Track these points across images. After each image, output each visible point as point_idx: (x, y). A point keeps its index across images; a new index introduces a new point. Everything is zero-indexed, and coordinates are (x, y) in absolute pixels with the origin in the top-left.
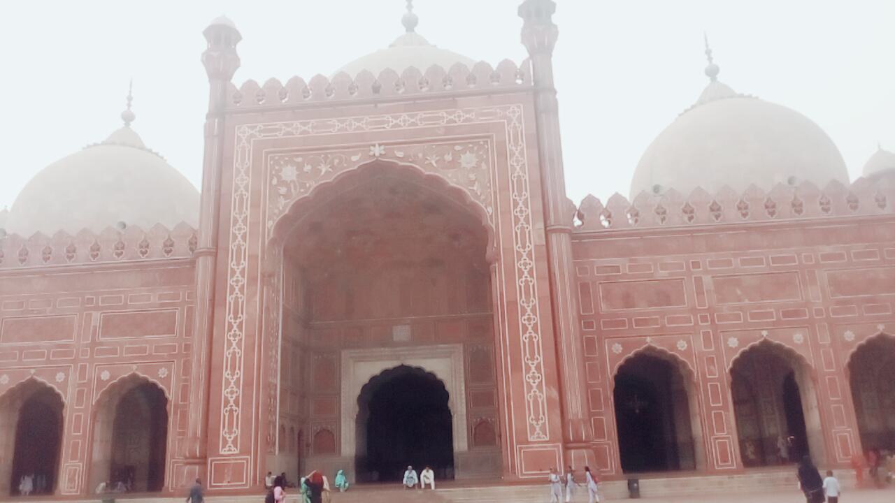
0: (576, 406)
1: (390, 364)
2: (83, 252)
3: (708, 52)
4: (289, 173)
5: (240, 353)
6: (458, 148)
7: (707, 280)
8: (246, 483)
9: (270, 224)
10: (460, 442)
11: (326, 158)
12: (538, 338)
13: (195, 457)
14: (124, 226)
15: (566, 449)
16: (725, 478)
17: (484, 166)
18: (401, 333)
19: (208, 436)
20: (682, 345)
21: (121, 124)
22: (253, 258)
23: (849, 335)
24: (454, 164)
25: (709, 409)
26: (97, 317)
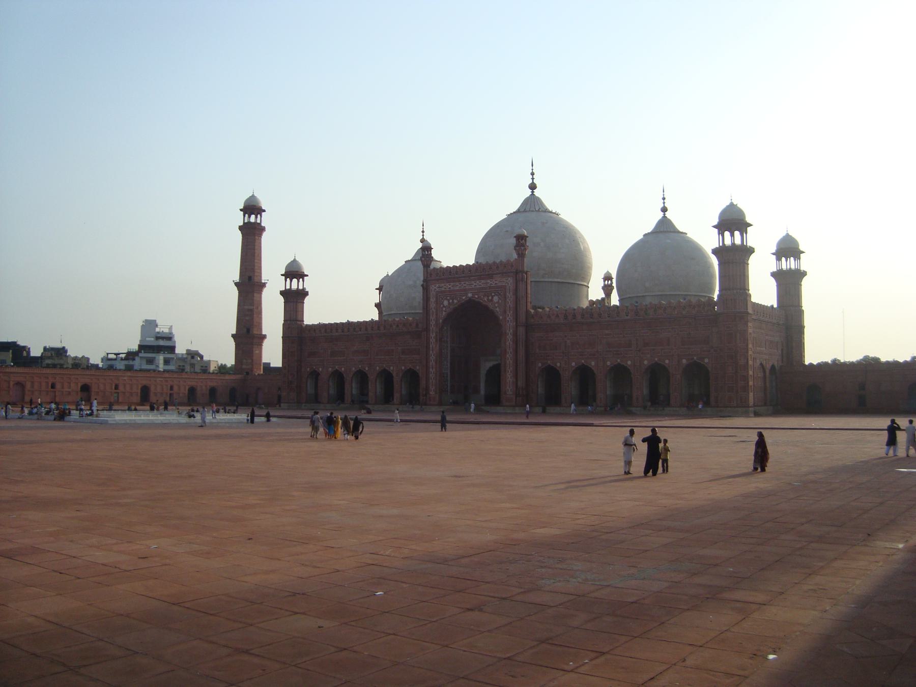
0: (521, 383)
3: (664, 199)
4: (446, 303)
19: (427, 389)
20: (558, 364)
24: (492, 300)
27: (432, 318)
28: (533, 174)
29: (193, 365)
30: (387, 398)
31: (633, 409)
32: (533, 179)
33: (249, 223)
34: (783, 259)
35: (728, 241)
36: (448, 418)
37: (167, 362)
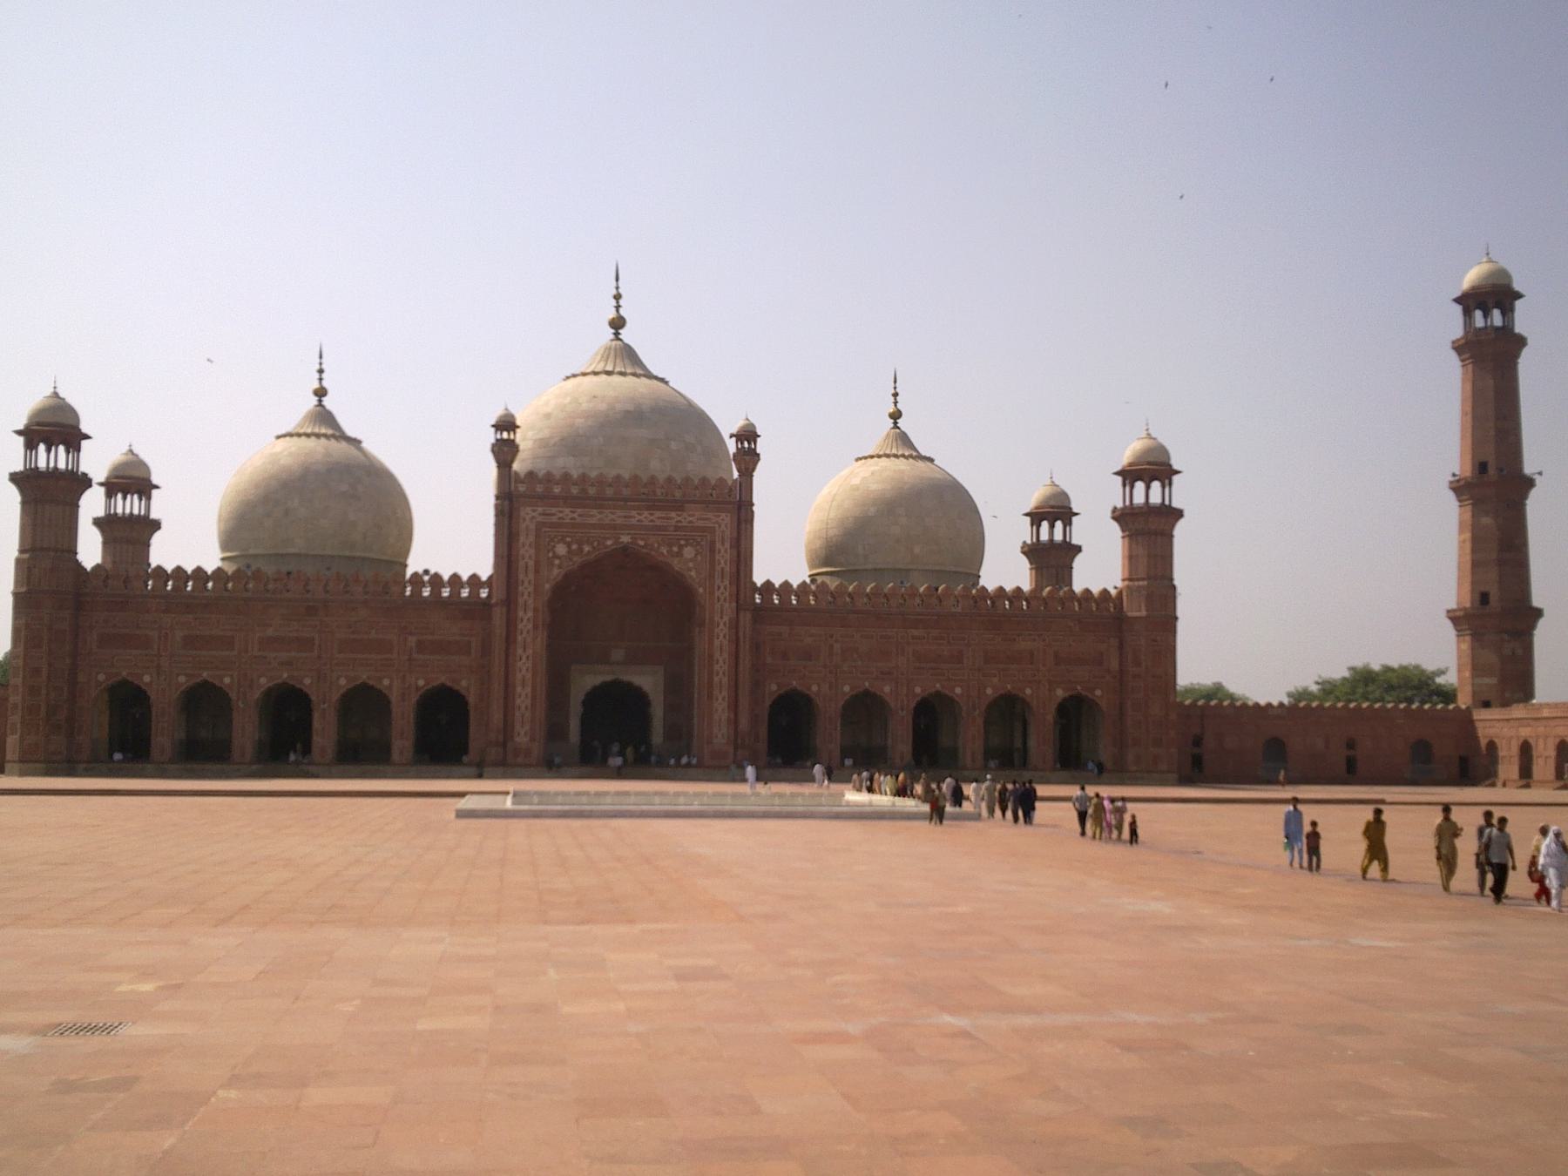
0: (744, 723)
1: (609, 678)
4: (561, 549)
5: (529, 676)
7: (837, 646)
9: (547, 586)
10: (657, 737)
12: (725, 680)
14: (426, 572)
15: (736, 749)
18: (618, 655)
19: (507, 729)
20: (815, 688)
21: (314, 400)
22: (536, 610)
23: (918, 690)
24: (679, 554)
26: (412, 640)
28: (618, 297)
32: (618, 307)
34: (1045, 525)
35: (1139, 498)
36: (1041, 790)
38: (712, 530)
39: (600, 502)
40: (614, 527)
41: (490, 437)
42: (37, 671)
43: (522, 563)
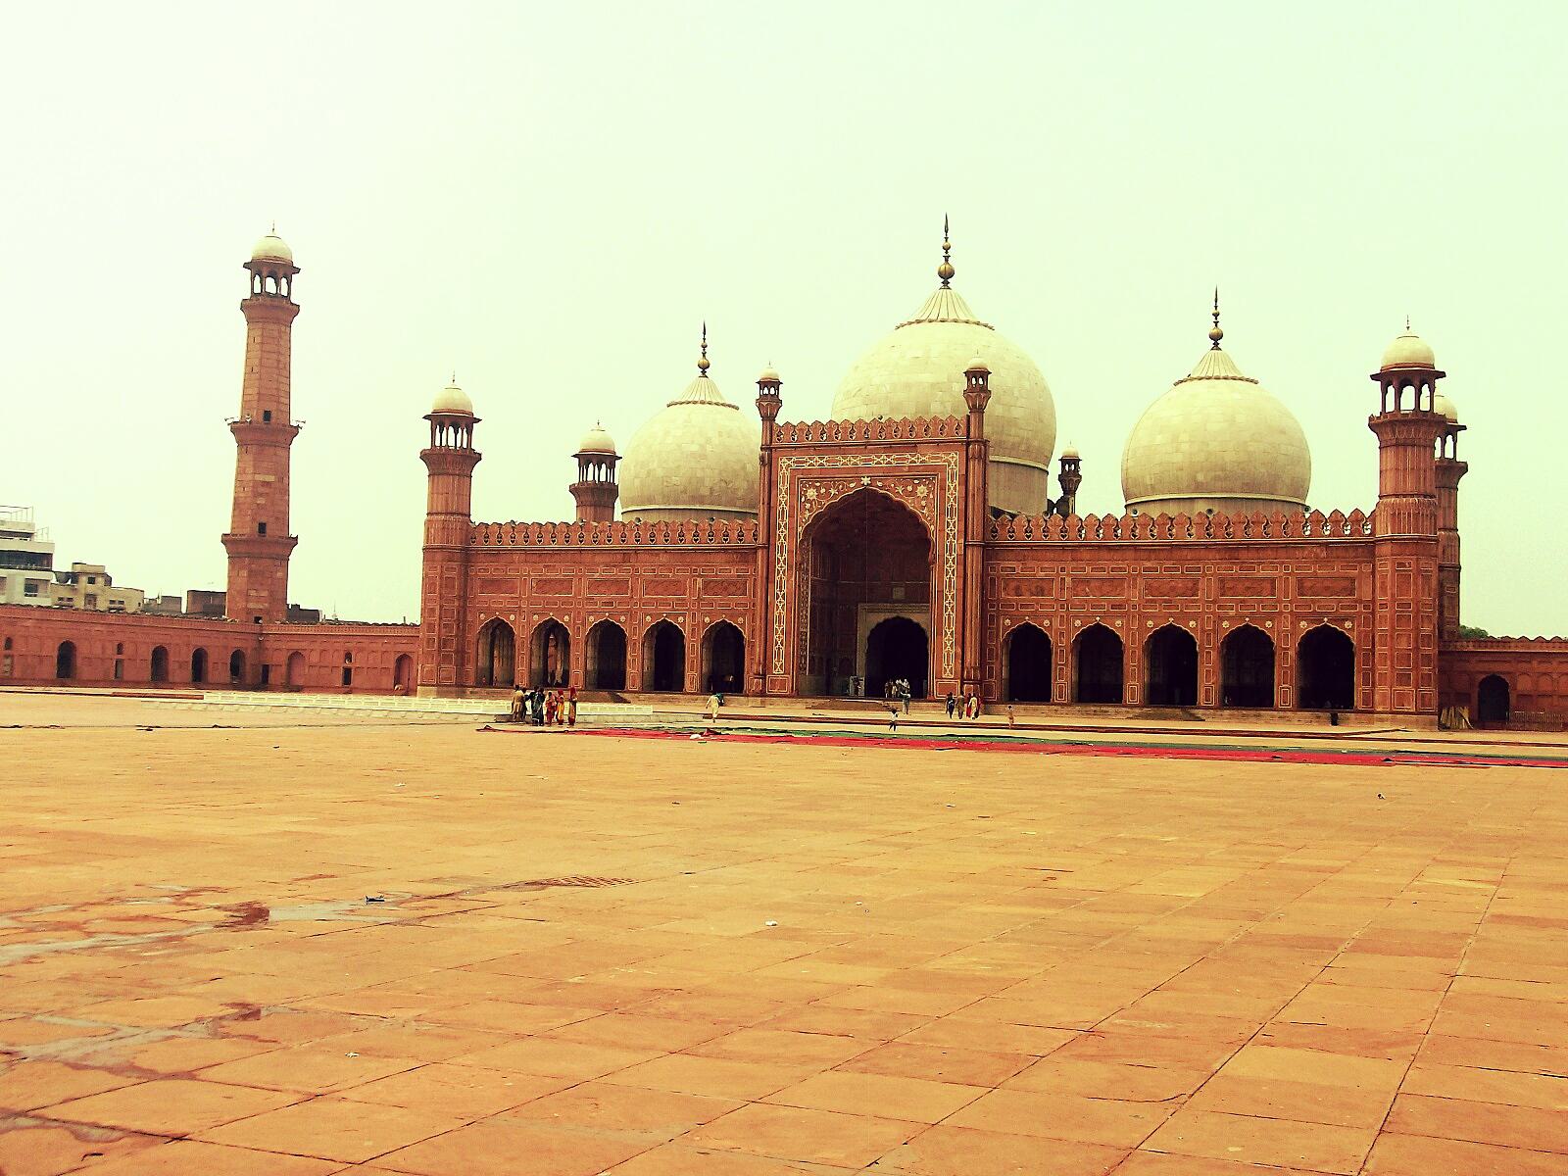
0: (971, 658)
2: (689, 537)
4: (811, 493)
6: (916, 482)
7: (1068, 580)
8: (787, 691)
11: (834, 484)
13: (759, 674)
15: (962, 684)
16: (1059, 708)
17: (931, 496)
18: (899, 593)
20: (1046, 622)
24: (913, 493)
25: (1057, 664)
27: (783, 522)
29: (91, 598)
30: (666, 679)
31: (1199, 713)
33: (263, 293)
37: (31, 588)
38: (942, 469)
39: (842, 449)
40: (856, 469)
41: (755, 392)
42: (433, 610)
43: (779, 508)
